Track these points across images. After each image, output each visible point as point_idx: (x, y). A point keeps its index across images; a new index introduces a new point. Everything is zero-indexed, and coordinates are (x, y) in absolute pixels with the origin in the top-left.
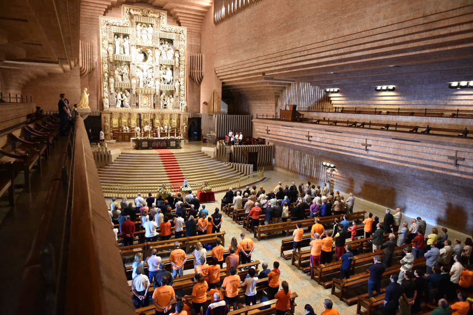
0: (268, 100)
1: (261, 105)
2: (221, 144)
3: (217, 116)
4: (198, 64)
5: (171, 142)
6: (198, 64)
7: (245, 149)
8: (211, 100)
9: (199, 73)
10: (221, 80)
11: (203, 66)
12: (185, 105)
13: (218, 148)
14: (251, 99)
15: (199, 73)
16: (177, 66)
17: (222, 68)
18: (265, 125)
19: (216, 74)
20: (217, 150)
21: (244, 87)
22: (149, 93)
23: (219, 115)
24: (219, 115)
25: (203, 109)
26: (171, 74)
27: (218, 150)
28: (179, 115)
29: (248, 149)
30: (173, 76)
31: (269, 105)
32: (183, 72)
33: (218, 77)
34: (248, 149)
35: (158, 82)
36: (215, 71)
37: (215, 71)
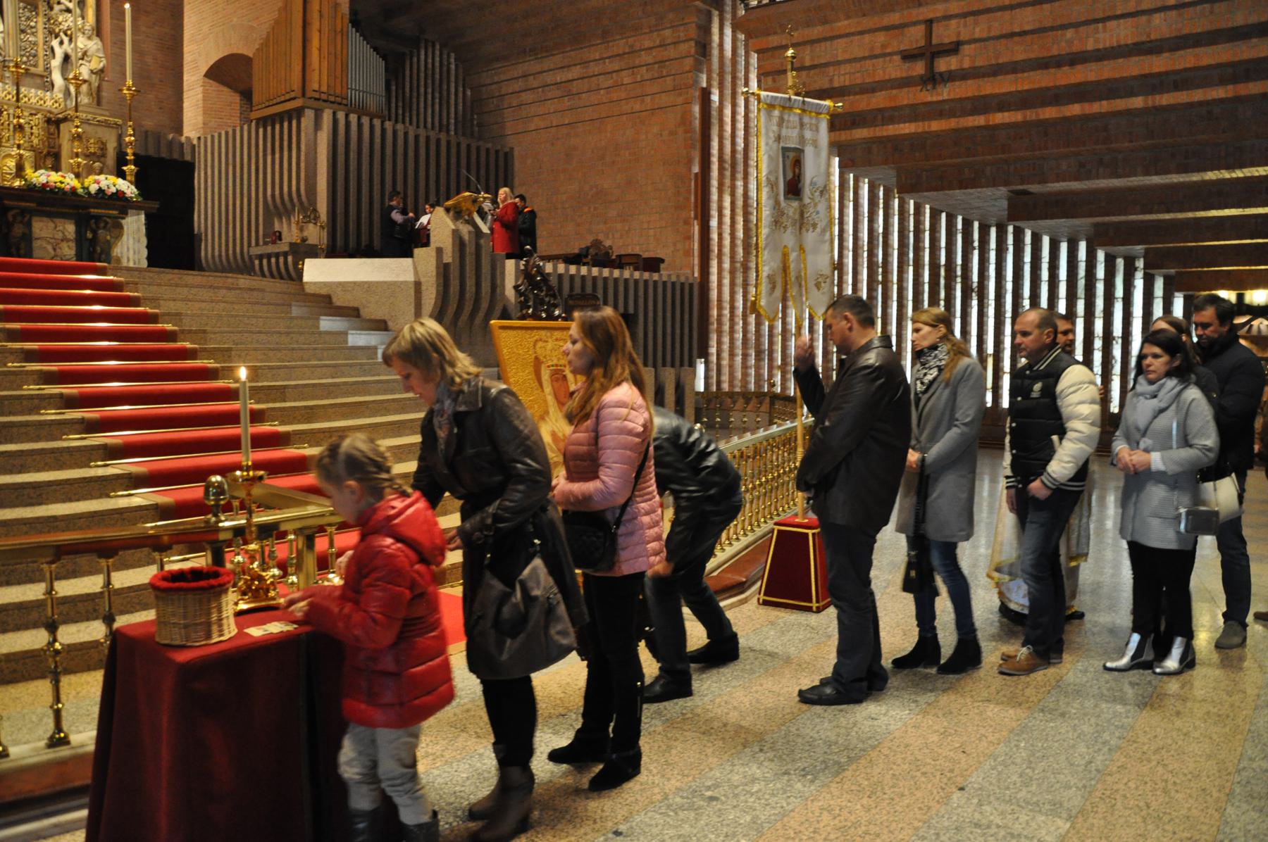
1: (575, 72)
2: (465, 230)
3: (327, 116)
5: (42, 229)
7: (578, 290)
8: (281, 23)
12: (96, 64)
13: (448, 258)
18: (895, 18)
20: (444, 271)
23: (341, 116)
24: (341, 116)
25: (208, 110)
27: (446, 266)
28: (54, 123)
29: (589, 290)
31: (646, 58)
34: (589, 290)
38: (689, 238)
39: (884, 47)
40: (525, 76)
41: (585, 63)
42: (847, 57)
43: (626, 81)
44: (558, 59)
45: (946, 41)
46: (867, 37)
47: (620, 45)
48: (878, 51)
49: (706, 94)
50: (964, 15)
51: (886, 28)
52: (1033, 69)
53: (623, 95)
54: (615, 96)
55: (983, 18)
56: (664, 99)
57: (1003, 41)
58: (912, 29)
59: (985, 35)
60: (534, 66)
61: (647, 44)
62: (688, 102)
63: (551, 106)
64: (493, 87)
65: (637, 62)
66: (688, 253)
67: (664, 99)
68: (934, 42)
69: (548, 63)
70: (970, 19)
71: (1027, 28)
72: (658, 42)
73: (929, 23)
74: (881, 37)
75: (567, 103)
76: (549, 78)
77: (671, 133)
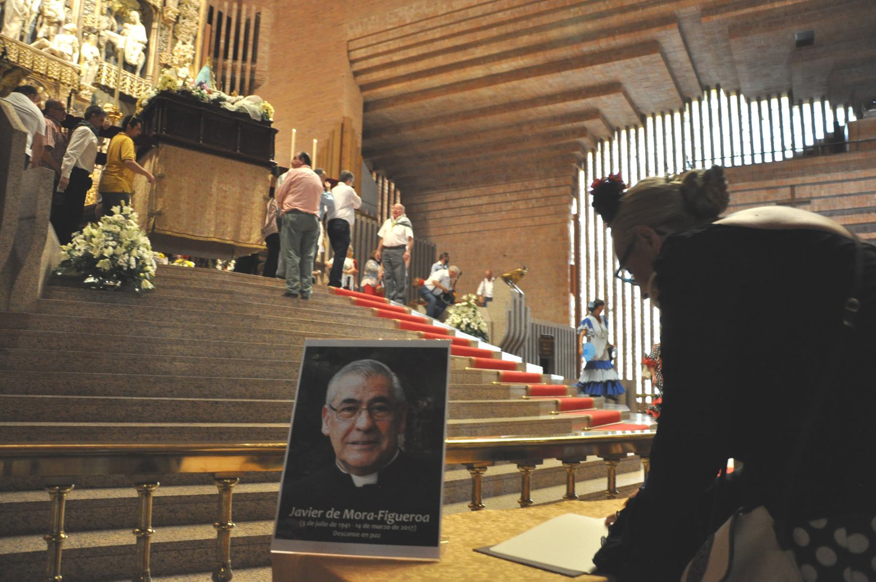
0: (531, 177)
1: (485, 200)
4: (242, 39)
6: (242, 39)
9: (243, 71)
10: (363, 88)
11: (264, 50)
14: (427, 188)
15: (243, 71)
16: (170, 14)
17: (408, 30)
19: (352, 62)
21: (455, 126)
22: (55, 74)
26: (146, 40)
30: (146, 51)
31: (535, 194)
32: (189, 45)
33: (356, 74)
35: (90, 49)
36: (349, 51)
37: (349, 51)
38: (567, 304)
39: (765, 198)
40: (447, 200)
41: (491, 195)
42: (742, 202)
43: (521, 207)
44: (473, 191)
45: (804, 197)
46: (754, 192)
47: (518, 186)
48: (762, 200)
49: (576, 218)
50: (814, 184)
51: (768, 188)
52: (852, 214)
53: (519, 215)
54: (513, 216)
55: (826, 186)
56: (548, 220)
57: (837, 198)
58: (782, 190)
59: (827, 195)
60: (454, 194)
61: (537, 185)
62: (566, 221)
63: (465, 220)
64: (422, 206)
65: (530, 196)
66: (567, 313)
67: (548, 220)
68: (797, 196)
69: (465, 193)
70: (817, 186)
71: (853, 192)
72: (545, 185)
73: (792, 187)
74: (764, 193)
75: (477, 218)
76: (464, 202)
77: (554, 240)
